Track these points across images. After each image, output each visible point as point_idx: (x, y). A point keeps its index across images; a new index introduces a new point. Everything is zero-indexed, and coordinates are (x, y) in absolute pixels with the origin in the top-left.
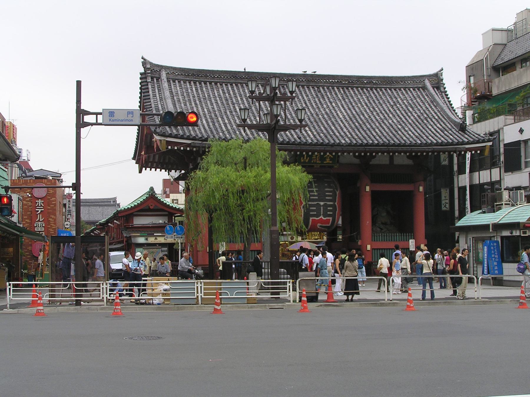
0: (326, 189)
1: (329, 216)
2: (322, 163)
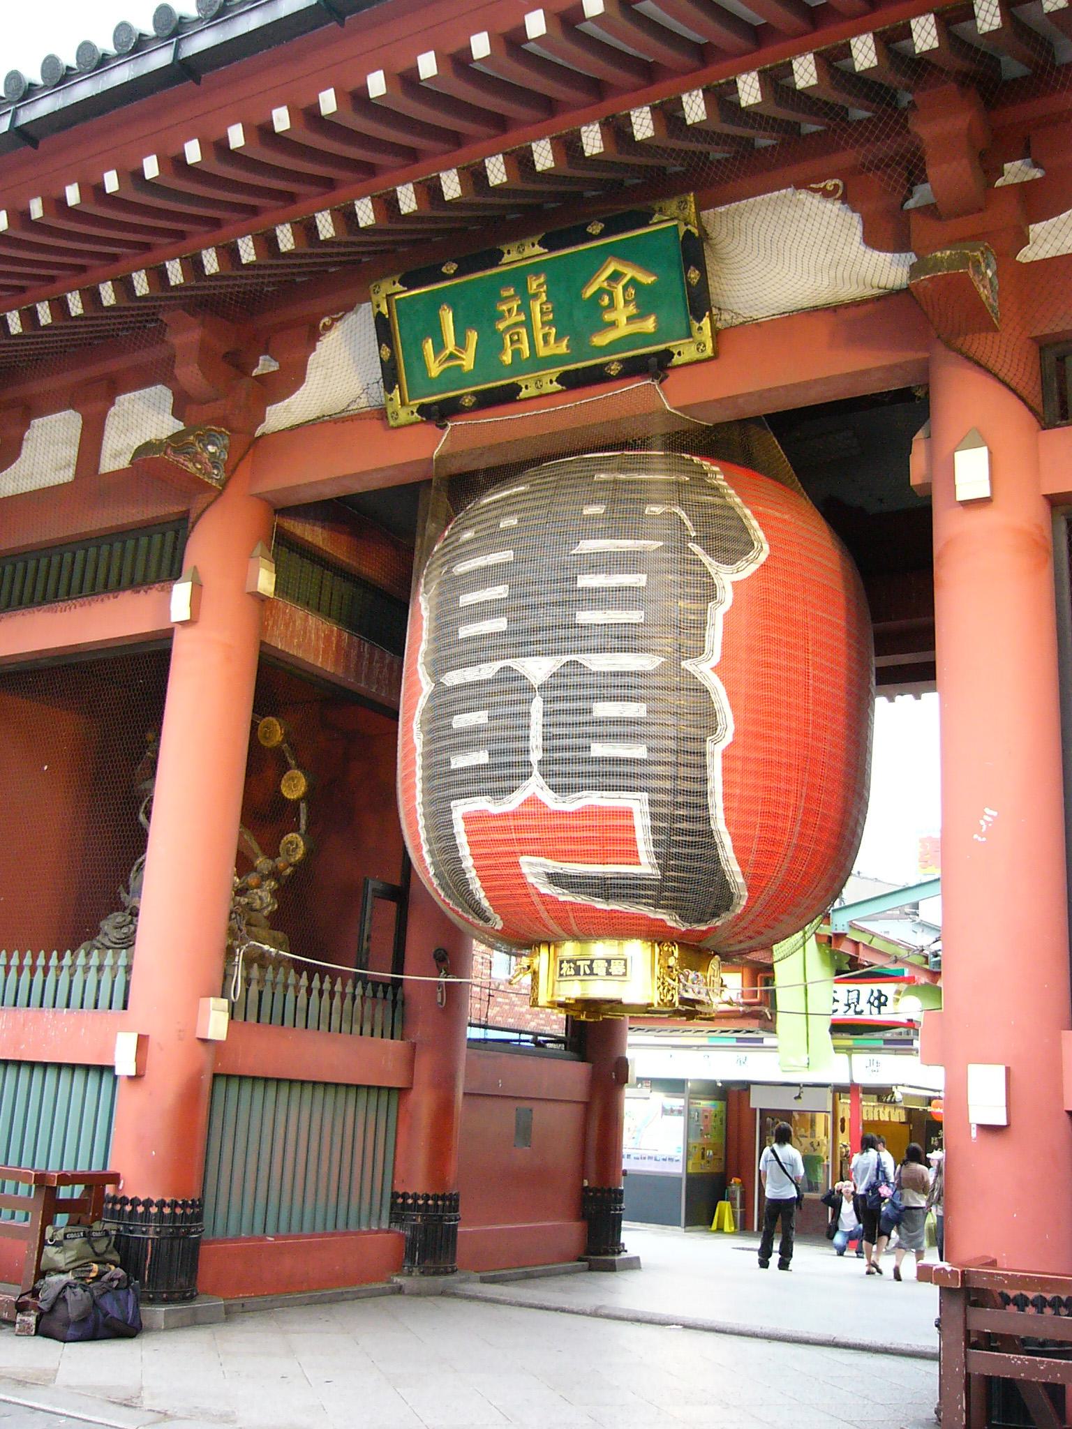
0: (588, 546)
1: (616, 775)
2: (580, 345)
